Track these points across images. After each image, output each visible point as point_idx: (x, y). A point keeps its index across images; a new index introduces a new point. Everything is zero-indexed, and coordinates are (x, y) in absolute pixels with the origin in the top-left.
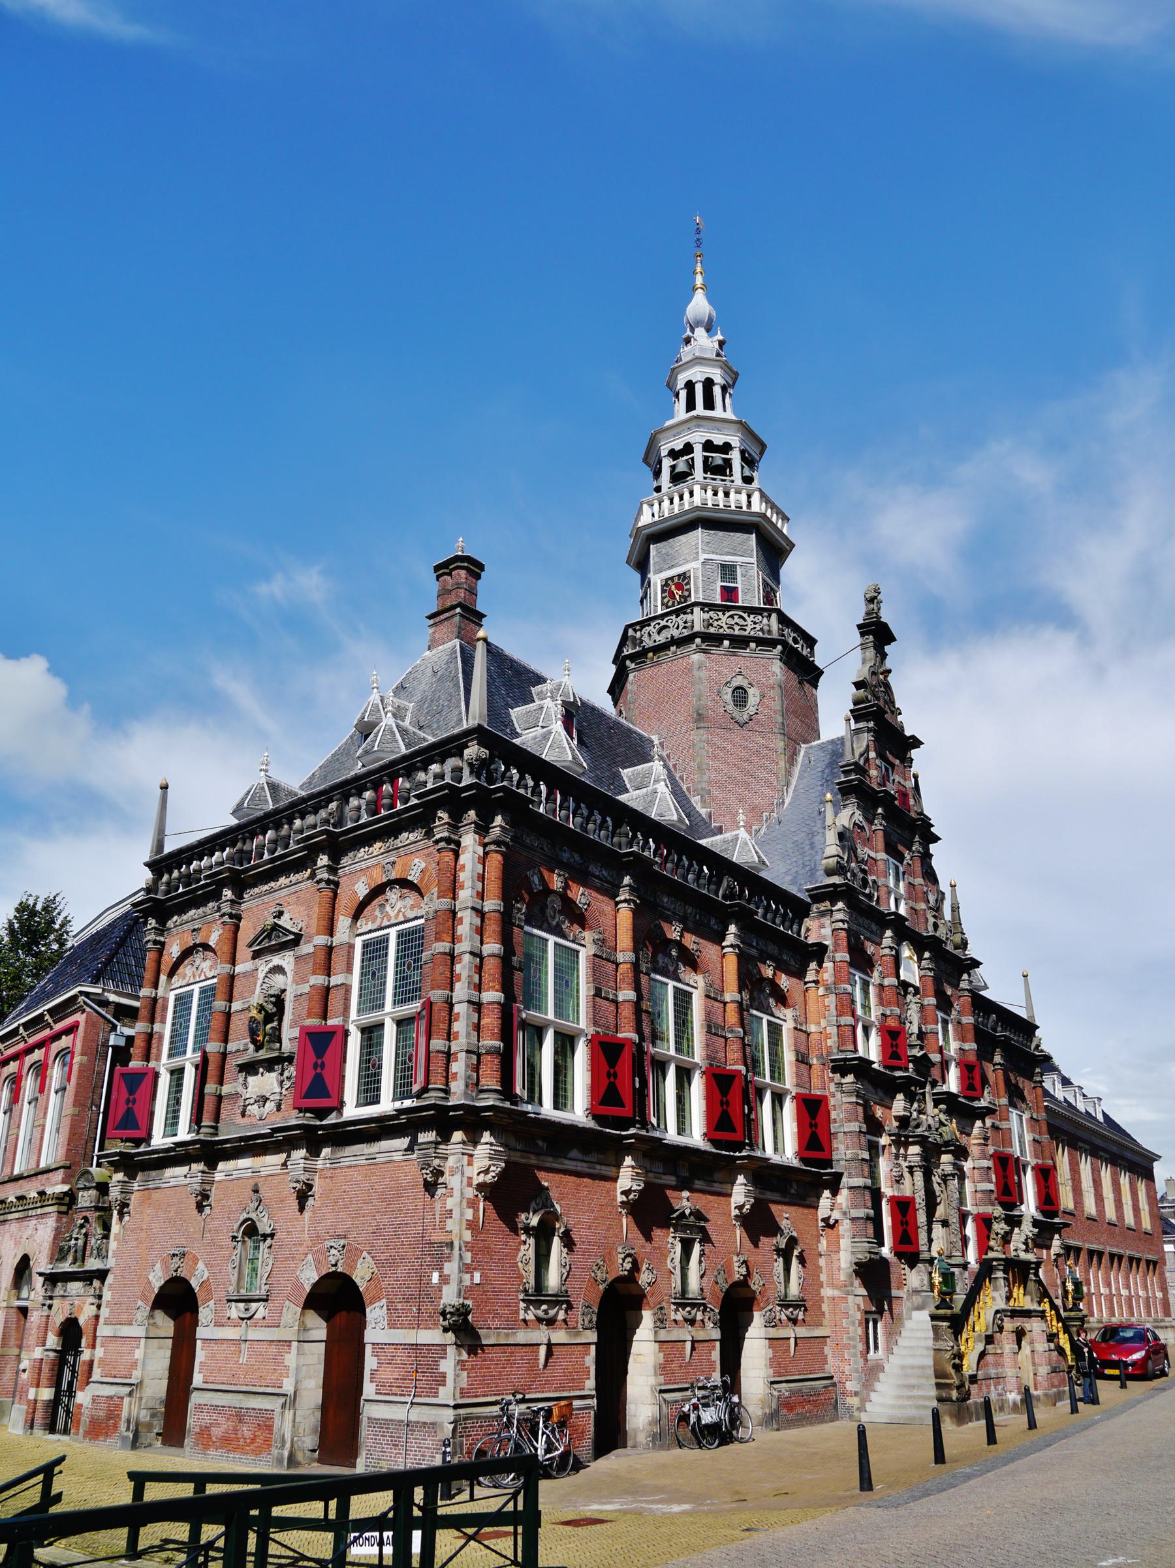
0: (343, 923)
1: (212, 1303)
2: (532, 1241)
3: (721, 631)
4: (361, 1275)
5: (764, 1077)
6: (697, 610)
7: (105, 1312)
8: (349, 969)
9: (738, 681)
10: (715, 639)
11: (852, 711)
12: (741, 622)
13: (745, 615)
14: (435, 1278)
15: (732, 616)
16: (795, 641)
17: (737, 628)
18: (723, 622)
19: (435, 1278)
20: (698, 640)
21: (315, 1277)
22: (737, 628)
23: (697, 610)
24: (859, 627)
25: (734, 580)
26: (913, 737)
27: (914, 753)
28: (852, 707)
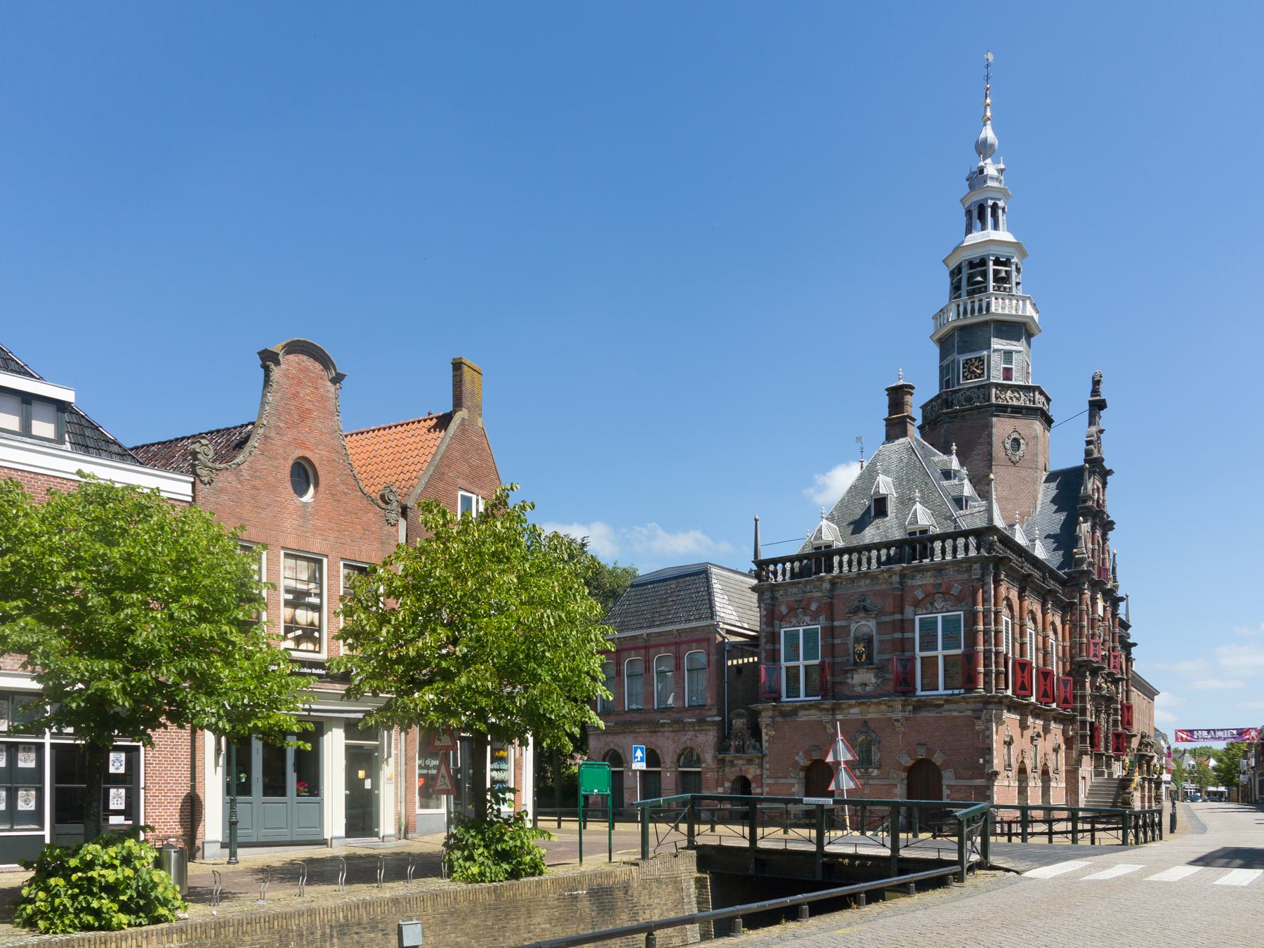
0: (909, 610)
4: (938, 759)
7: (766, 773)
9: (1015, 435)
14: (981, 761)
18: (1010, 398)
19: (981, 761)
25: (1011, 363)
27: (1109, 478)
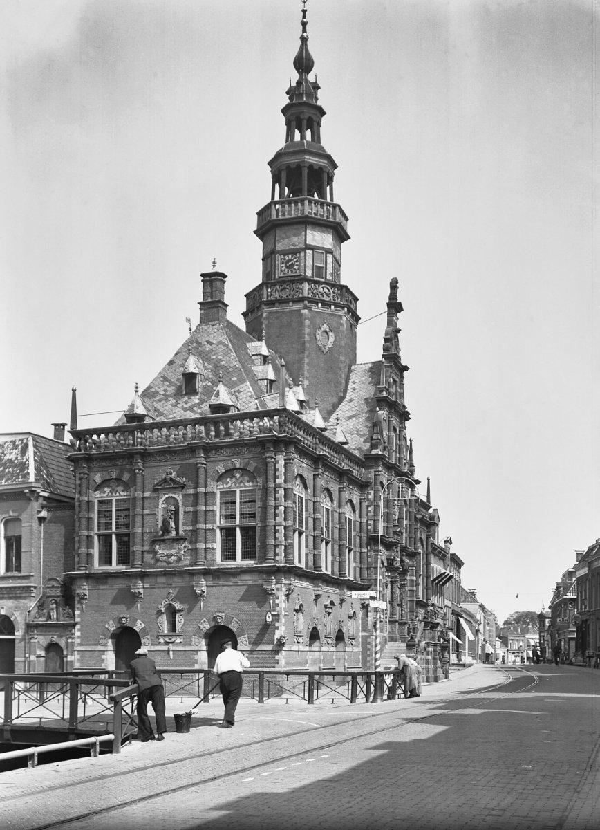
1: (149, 637)
4: (233, 626)
8: (214, 504)
20: (306, 302)
21: (208, 627)
26: (406, 366)
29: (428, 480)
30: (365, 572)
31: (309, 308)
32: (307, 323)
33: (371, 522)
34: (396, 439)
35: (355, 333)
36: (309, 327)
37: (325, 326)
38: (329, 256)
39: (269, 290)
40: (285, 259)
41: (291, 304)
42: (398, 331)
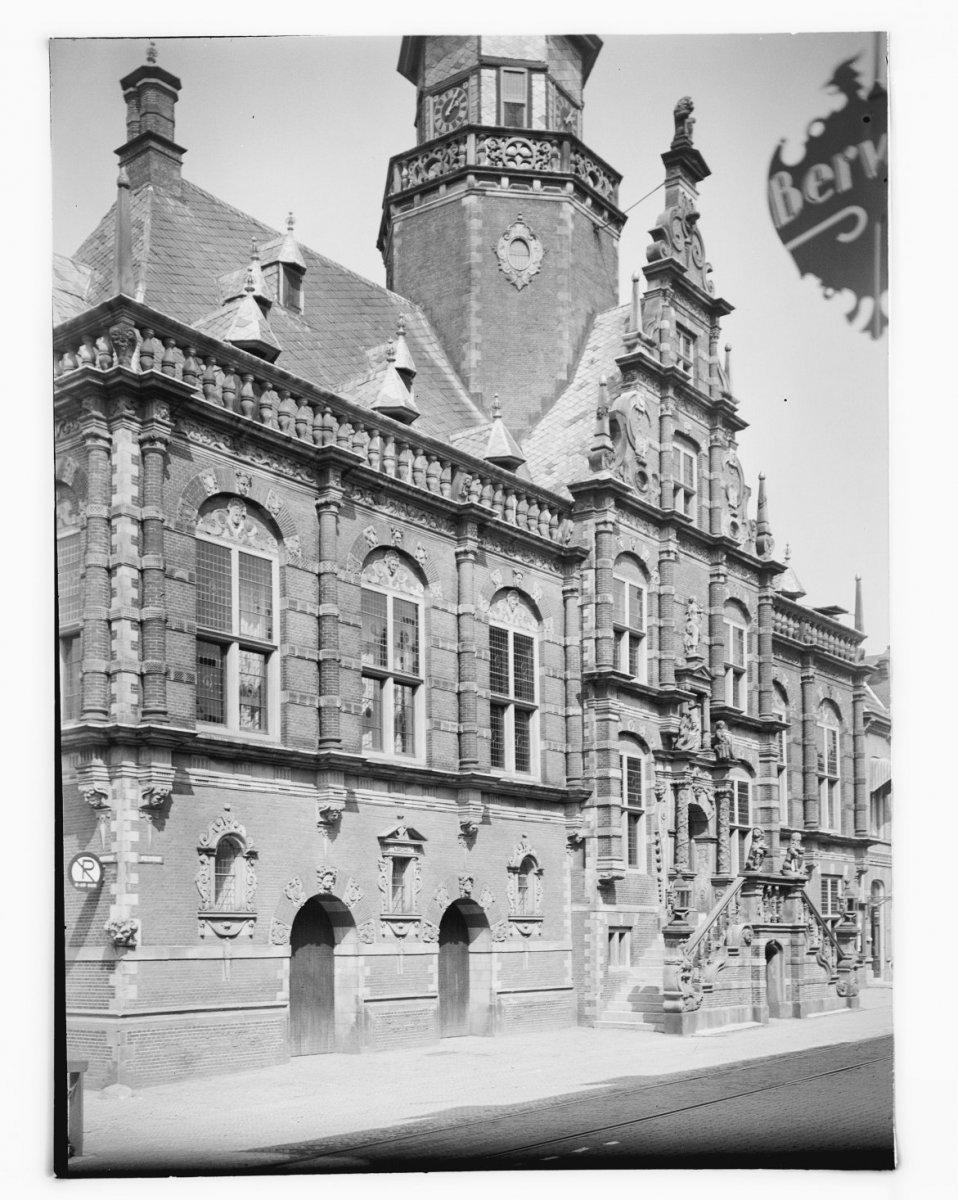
2: (213, 859)
3: (500, 165)
5: (507, 692)
6: (472, 138)
10: (492, 175)
11: (645, 269)
12: (525, 151)
13: (530, 143)
15: (513, 144)
16: (592, 175)
17: (519, 159)
20: (471, 178)
22: (519, 159)
23: (472, 138)
24: (665, 157)
28: (646, 263)
29: (858, 580)
30: (577, 761)
31: (481, 192)
32: (475, 224)
33: (590, 644)
34: (700, 466)
35: (615, 251)
36: (481, 233)
37: (519, 227)
38: (539, 81)
39: (405, 172)
40: (441, 103)
41: (442, 189)
42: (693, 218)
